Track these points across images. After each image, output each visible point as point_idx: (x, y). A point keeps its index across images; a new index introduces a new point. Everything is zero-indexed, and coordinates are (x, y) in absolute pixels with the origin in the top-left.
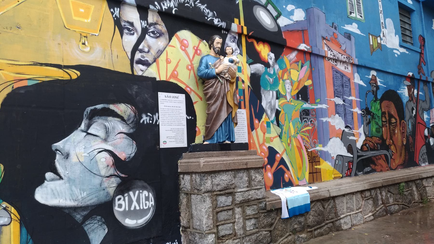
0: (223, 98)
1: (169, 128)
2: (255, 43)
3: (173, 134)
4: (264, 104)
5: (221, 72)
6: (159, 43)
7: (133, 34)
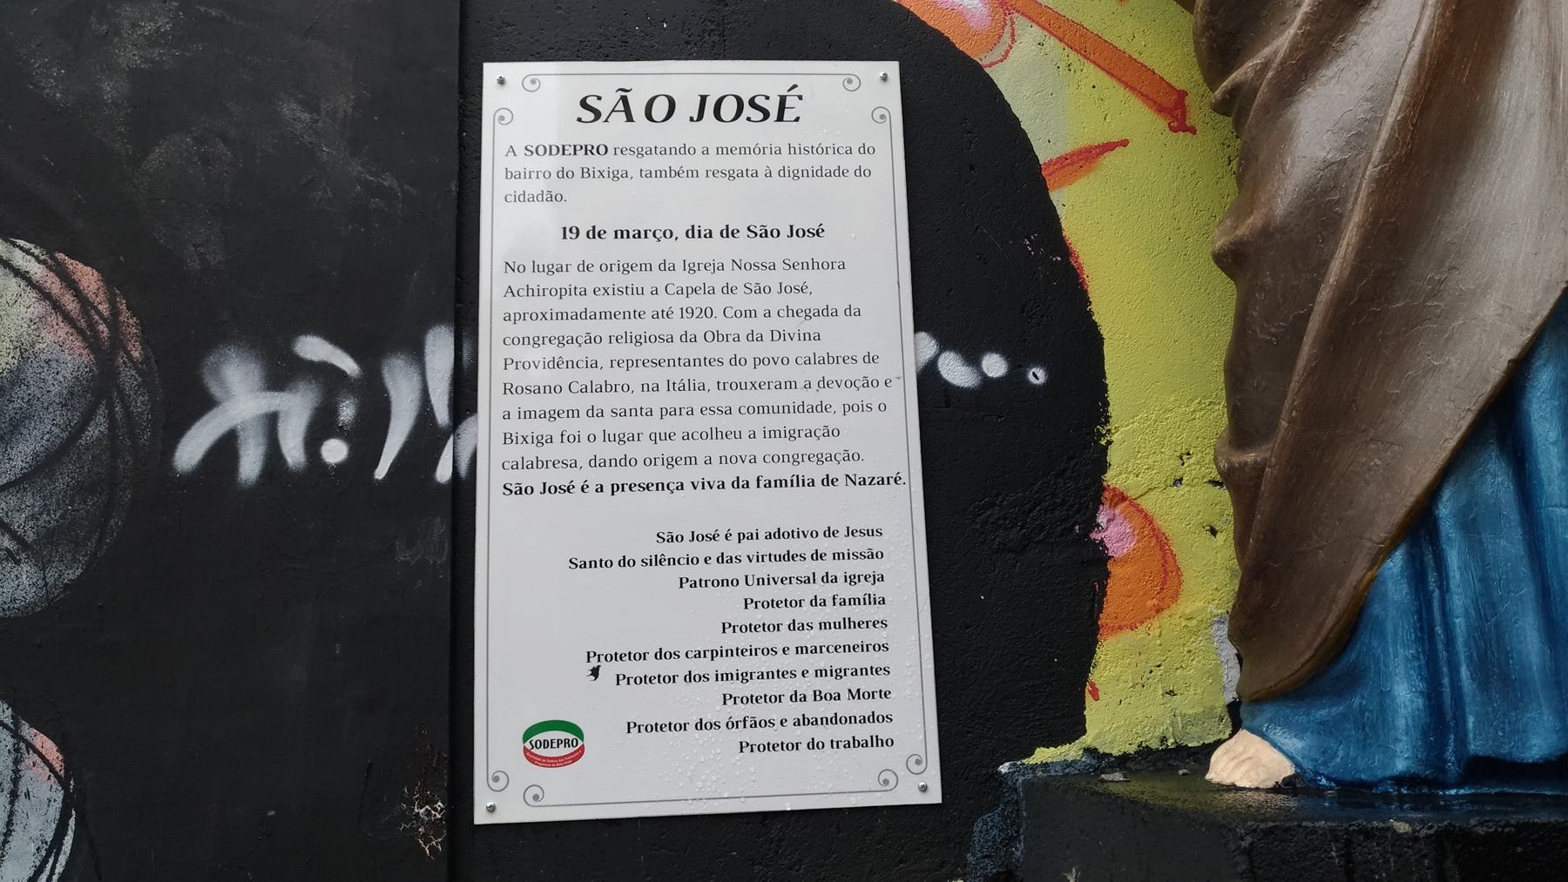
1: (633, 523)
3: (698, 619)
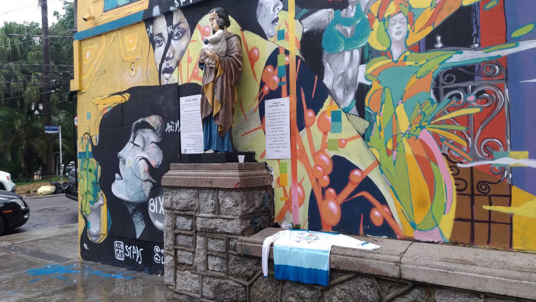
1: (188, 135)
4: (328, 81)
6: (182, 43)
7: (162, 45)
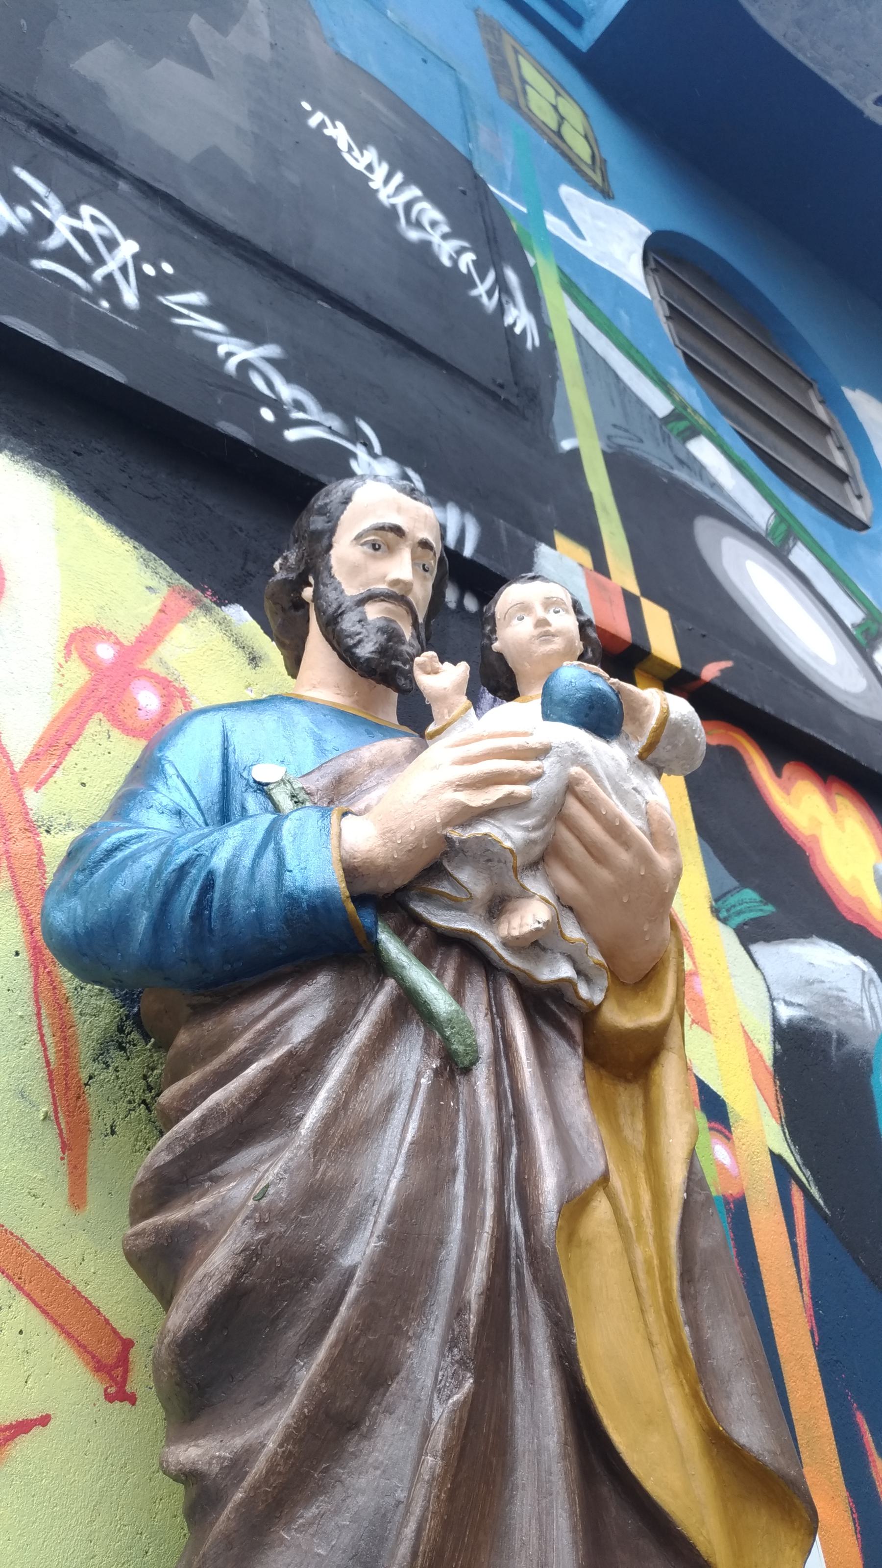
0: (490, 1350)
2: (759, 766)
5: (434, 863)
